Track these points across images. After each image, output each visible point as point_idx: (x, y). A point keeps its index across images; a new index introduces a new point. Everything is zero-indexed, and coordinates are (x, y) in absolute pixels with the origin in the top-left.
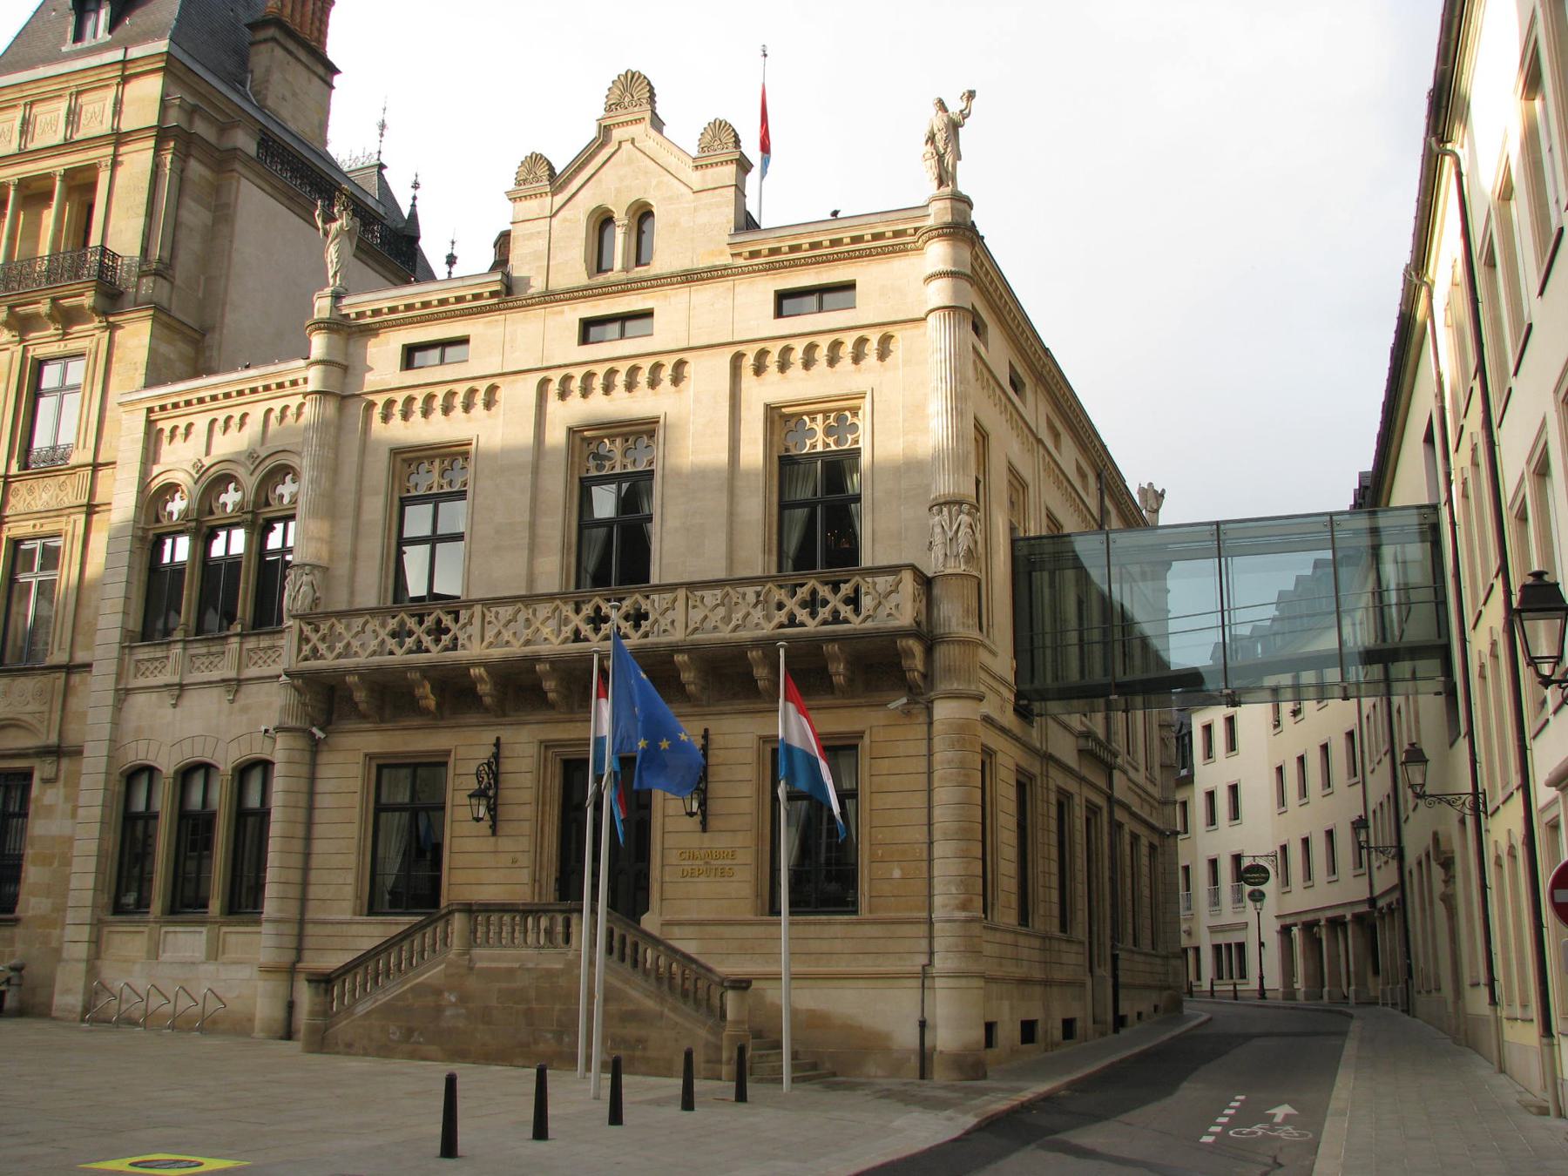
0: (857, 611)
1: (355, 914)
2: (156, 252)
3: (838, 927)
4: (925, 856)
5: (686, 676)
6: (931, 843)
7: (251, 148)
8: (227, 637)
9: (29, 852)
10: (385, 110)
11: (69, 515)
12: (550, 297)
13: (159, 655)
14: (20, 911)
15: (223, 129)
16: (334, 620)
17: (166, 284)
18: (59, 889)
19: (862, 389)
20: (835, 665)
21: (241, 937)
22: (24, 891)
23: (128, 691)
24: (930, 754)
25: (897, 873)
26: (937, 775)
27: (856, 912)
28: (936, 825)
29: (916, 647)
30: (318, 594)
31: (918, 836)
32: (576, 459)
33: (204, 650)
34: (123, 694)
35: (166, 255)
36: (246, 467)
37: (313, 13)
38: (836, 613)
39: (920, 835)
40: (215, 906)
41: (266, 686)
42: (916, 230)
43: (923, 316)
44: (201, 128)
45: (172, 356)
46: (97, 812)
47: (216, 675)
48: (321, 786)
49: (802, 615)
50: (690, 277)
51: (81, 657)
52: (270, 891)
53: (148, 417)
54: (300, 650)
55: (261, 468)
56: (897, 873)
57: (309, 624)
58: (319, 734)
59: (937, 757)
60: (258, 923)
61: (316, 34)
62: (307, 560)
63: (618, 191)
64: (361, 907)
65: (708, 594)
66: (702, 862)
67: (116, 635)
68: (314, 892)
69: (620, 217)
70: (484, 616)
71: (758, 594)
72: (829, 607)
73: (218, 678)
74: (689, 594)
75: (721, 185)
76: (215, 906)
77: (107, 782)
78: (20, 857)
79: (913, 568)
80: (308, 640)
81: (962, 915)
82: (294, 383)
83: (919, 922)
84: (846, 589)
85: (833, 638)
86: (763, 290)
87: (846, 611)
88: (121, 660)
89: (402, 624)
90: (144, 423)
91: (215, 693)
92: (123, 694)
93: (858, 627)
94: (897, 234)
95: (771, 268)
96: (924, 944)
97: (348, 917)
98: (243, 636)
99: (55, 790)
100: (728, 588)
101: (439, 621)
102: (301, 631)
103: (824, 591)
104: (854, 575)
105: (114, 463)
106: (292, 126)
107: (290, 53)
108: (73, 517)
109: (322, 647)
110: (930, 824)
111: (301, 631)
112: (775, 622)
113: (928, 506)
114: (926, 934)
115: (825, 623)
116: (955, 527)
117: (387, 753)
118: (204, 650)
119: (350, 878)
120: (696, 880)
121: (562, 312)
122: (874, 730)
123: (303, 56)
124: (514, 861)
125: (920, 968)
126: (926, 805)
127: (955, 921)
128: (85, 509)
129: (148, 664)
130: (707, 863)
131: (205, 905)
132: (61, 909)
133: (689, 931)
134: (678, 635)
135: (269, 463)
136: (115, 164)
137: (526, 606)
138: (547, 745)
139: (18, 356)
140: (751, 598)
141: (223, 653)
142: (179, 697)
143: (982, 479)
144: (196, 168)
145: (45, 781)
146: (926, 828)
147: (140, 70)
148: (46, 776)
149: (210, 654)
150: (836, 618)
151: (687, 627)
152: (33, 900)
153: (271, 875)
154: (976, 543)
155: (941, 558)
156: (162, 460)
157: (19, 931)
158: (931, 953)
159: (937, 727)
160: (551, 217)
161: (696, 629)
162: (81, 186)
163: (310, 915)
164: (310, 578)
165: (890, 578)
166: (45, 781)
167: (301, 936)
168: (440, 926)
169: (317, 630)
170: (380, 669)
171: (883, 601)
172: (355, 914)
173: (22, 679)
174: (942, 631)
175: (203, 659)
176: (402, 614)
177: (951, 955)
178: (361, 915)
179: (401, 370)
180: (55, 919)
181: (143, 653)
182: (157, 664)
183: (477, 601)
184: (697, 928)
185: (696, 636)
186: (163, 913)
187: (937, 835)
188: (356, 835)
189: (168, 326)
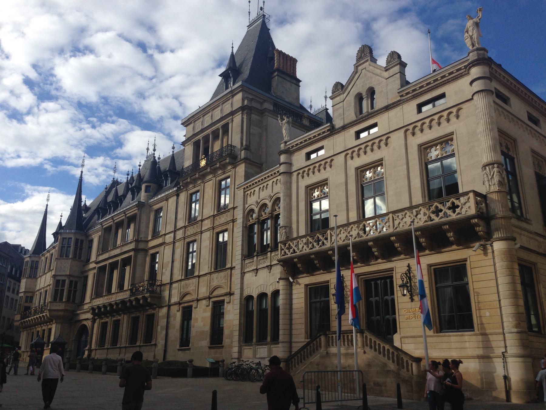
0: (454, 212)
1: (305, 339)
2: (244, 143)
3: (466, 337)
4: (498, 306)
5: (397, 245)
6: (500, 301)
7: (271, 107)
8: (267, 252)
9: (225, 325)
10: (326, 92)
11: (229, 223)
12: (344, 128)
13: (251, 261)
14: (223, 344)
15: (262, 104)
16: (289, 242)
17: (248, 152)
18: (231, 336)
19: (452, 131)
20: (449, 234)
21: (276, 348)
22: (224, 336)
23: (244, 273)
24: (495, 265)
25: (488, 314)
26: (498, 272)
27: (474, 331)
28: (500, 293)
29: (481, 223)
30: (288, 235)
31: (494, 298)
32: (359, 178)
33: (262, 258)
34: (243, 274)
35: (248, 143)
36: (268, 200)
37: (290, 65)
38: (445, 214)
39: (496, 297)
40: (269, 339)
42: (464, 66)
43: (471, 97)
44: (254, 104)
45: (253, 172)
46: (238, 311)
47: (265, 265)
48: (294, 296)
49: (433, 216)
50: (387, 108)
51: (233, 266)
52: (281, 332)
53: (244, 191)
54: (281, 253)
55: (272, 199)
56: (488, 314)
57: (283, 244)
58: (292, 280)
59: (497, 265)
60: (278, 343)
61: (292, 71)
62: (284, 225)
64: (307, 336)
65: (400, 214)
66: (412, 313)
67: (240, 257)
68: (294, 332)
70: (331, 234)
71: (417, 212)
72: (443, 212)
73: (265, 266)
74: (393, 215)
75: (394, 74)
76: (269, 339)
77: (240, 301)
78: (223, 327)
79: (474, 192)
80: (283, 249)
81: (515, 330)
82: (278, 172)
83: (500, 334)
84: (449, 204)
85: (445, 224)
86: (413, 104)
87: (449, 212)
88: (242, 264)
90: (243, 193)
91: (266, 270)
92: (243, 274)
93: (455, 217)
94: (458, 70)
95: (415, 97)
96: (502, 343)
98: (271, 252)
99: (230, 306)
100: (406, 211)
101: (318, 237)
103: (440, 206)
104: (451, 198)
105: (237, 207)
106: (286, 100)
107: (283, 78)
108: (230, 224)
109: (287, 251)
110: (498, 293)
111: (281, 247)
113: (482, 167)
114: (503, 339)
115: (441, 218)
116: (492, 174)
117: (312, 283)
118: (262, 258)
119: (303, 327)
120: (411, 320)
121: (349, 131)
122: (471, 257)
123: (288, 78)
125: (501, 353)
126: (496, 285)
127: (513, 333)
128: (232, 221)
129: (249, 264)
130: (414, 314)
131: (266, 339)
132: (232, 342)
133: (411, 340)
134: (391, 230)
136: (232, 121)
137: (343, 228)
139: (214, 180)
140: (415, 213)
141: (267, 258)
142: (257, 273)
143: (515, 156)
144: (254, 117)
145: (228, 303)
146: (497, 294)
147: (236, 92)
148: (228, 301)
149: (264, 259)
150: (446, 215)
151: (394, 226)
152: (227, 340)
153: (281, 327)
154: (503, 178)
155: (488, 187)
156: (248, 202)
157: (224, 350)
158: (506, 347)
159: (496, 253)
160: (343, 101)
161: (397, 228)
162: (226, 129)
163: (294, 340)
164: (285, 230)
165: (466, 197)
166: (228, 303)
167: (291, 347)
168: (318, 340)
169: (285, 246)
171: (463, 206)
172: (305, 339)
173: (221, 273)
174: (492, 215)
175: (262, 261)
176: (308, 237)
177: (513, 347)
178: (307, 339)
179: (306, 161)
180: (231, 347)
181: (247, 261)
182: (251, 264)
184: (413, 339)
185: (398, 229)
186: (256, 342)
187: (501, 298)
188: (304, 312)
189: (249, 164)
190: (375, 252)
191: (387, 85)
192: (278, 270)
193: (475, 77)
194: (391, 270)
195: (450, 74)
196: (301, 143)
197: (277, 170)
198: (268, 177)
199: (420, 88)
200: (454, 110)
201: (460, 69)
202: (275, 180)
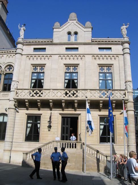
41: (5, 101)
42: (122, 41)
54: (16, 95)
60: (4, 142)
63: (72, 30)
69: (72, 33)
89: (37, 92)
95: (98, 44)
97: (22, 142)
102: (17, 92)
111: (17, 92)
112: (105, 96)
124: (54, 133)
135: (7, 64)
138: (60, 114)
170: (32, 100)
183: (51, 89)
190: (76, 105)
191: (85, 34)
192: (12, 104)
193: (126, 47)
194: (80, 114)
195: (115, 42)
196: (32, 42)
197: (12, 51)
198: (5, 52)
199: (102, 41)
200: (115, 56)
201: (120, 42)
202: (9, 55)
